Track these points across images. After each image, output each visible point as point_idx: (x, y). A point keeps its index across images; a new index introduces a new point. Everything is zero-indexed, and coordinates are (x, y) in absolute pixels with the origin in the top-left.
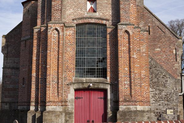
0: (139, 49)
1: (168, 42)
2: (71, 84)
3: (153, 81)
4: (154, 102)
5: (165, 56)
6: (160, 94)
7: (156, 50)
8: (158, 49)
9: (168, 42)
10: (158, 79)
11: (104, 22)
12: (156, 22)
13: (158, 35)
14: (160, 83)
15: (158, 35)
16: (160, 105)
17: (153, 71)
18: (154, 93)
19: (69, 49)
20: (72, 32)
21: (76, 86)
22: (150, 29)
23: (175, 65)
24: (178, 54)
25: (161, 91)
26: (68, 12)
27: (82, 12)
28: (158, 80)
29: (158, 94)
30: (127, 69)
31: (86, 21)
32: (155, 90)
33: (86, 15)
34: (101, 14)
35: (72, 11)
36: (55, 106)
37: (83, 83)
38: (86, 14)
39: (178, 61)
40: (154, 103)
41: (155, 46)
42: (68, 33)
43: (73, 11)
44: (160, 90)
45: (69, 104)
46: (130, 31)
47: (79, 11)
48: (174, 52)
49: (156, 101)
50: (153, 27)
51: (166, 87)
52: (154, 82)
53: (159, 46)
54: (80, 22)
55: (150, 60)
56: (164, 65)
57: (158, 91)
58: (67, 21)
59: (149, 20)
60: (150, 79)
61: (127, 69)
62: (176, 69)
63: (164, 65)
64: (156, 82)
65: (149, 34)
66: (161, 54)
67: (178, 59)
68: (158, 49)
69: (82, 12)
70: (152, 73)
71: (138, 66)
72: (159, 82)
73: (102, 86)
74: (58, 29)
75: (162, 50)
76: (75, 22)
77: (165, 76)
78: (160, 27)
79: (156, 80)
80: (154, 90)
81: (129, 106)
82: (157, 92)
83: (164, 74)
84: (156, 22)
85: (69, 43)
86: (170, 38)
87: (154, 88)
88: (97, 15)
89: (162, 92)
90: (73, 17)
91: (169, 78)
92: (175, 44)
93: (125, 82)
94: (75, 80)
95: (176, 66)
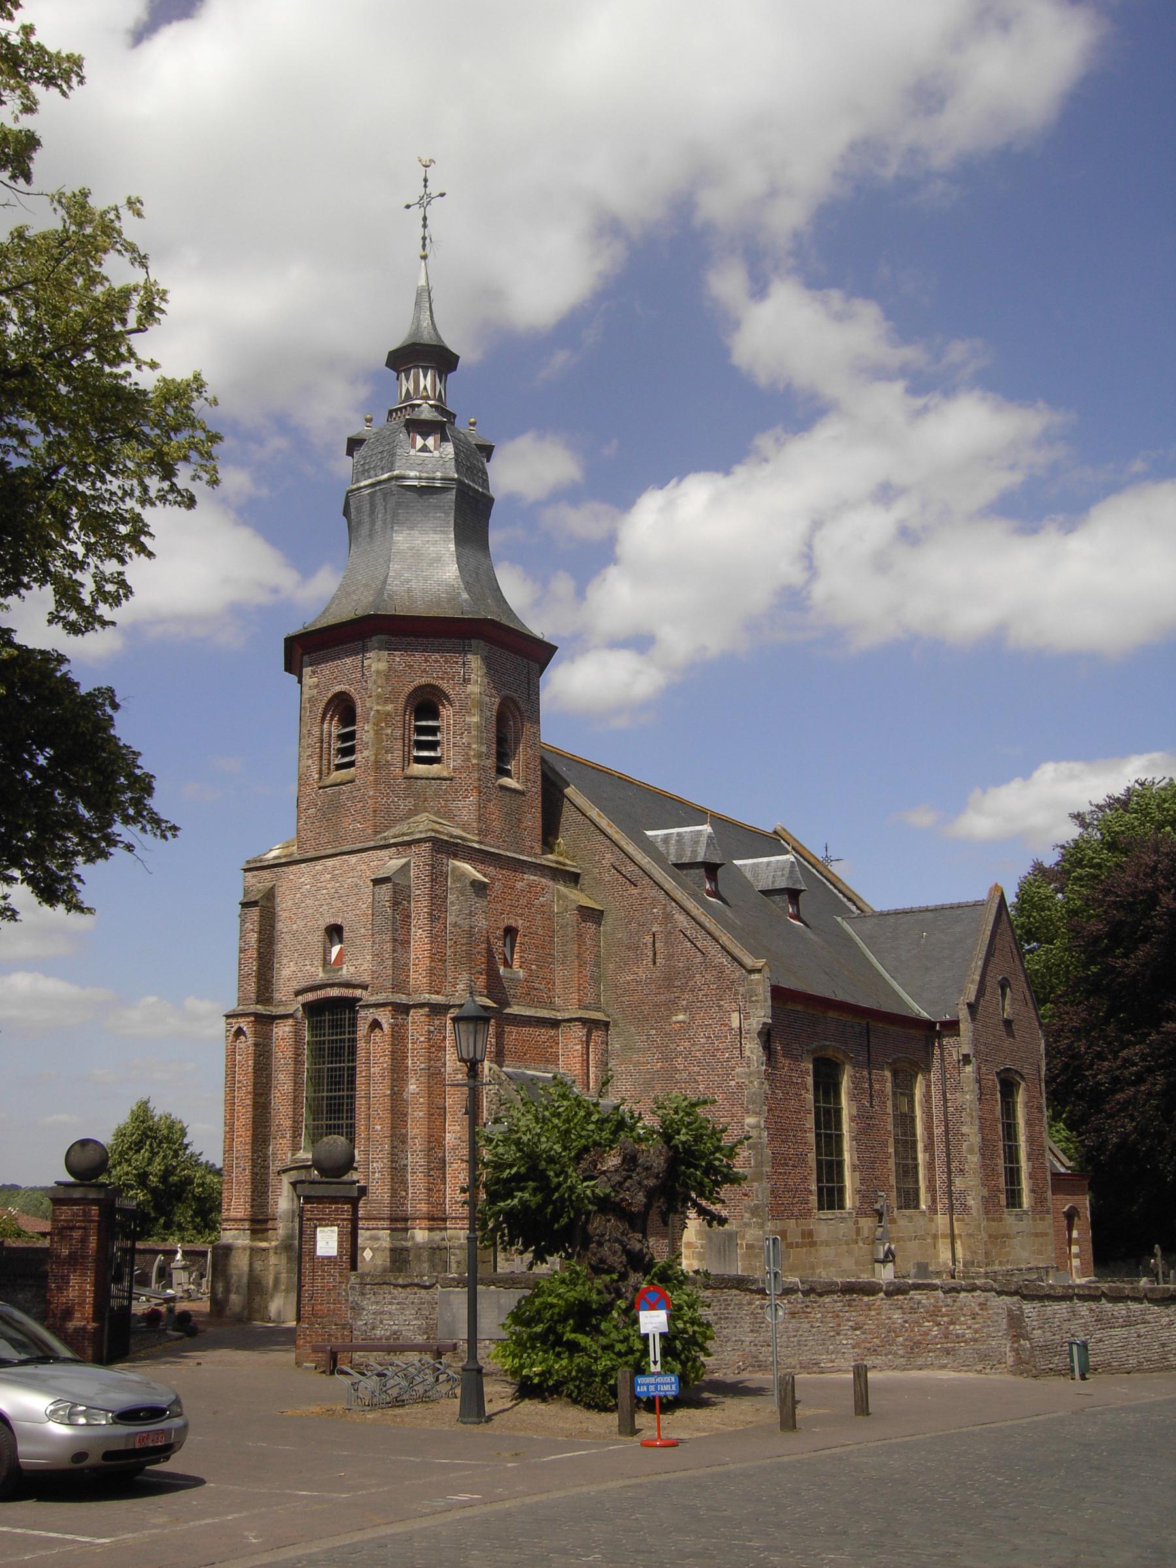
2: (285, 1171)
8: (681, 1017)
11: (358, 993)
12: (676, 916)
19: (281, 1077)
20: (287, 1029)
21: (294, 1175)
23: (738, 1070)
24: (747, 1027)
26: (286, 973)
31: (321, 994)
33: (321, 975)
34: (352, 969)
38: (321, 975)
39: (747, 1053)
41: (671, 1006)
42: (280, 1033)
48: (735, 1024)
53: (684, 1003)
54: (310, 997)
56: (699, 1074)
58: (284, 999)
63: (699, 1074)
65: (654, 963)
71: (421, 1114)
75: (693, 1019)
76: (300, 998)
78: (688, 933)
84: (676, 916)
86: (720, 969)
90: (296, 985)
92: (736, 994)
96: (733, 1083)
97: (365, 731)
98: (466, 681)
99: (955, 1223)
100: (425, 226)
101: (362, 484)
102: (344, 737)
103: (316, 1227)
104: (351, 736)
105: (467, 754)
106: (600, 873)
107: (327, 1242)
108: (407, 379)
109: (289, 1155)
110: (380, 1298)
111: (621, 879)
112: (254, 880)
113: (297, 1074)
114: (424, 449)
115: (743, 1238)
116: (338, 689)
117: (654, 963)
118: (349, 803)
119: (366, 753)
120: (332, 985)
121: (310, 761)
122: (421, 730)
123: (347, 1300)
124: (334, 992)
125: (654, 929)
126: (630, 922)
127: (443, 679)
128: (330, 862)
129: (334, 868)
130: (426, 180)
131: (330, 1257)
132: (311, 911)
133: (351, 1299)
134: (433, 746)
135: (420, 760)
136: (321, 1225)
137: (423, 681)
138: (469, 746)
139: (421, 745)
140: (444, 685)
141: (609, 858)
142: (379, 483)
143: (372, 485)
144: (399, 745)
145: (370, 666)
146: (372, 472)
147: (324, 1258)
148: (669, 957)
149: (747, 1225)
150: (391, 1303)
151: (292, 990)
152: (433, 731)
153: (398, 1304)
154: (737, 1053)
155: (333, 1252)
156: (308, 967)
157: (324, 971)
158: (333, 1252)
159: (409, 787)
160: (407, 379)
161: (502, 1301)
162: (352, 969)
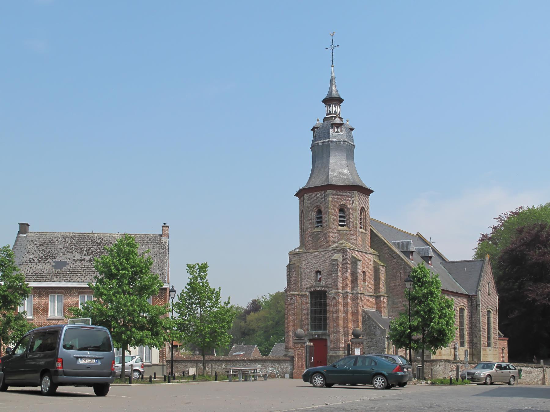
11: (326, 289)
25: (373, 339)
31: (315, 289)
37: (312, 335)
49: (369, 347)
54: (311, 290)
73: (324, 337)
76: (308, 290)
79: (368, 330)
82: (370, 340)
88: (322, 283)
97: (325, 217)
98: (353, 203)
102: (318, 218)
104: (321, 218)
113: (308, 311)
114: (337, 132)
119: (326, 224)
122: (340, 217)
124: (318, 289)
128: (316, 254)
135: (341, 225)
137: (341, 203)
139: (341, 221)
142: (325, 142)
143: (323, 142)
144: (335, 221)
155: (359, 354)
158: (359, 354)
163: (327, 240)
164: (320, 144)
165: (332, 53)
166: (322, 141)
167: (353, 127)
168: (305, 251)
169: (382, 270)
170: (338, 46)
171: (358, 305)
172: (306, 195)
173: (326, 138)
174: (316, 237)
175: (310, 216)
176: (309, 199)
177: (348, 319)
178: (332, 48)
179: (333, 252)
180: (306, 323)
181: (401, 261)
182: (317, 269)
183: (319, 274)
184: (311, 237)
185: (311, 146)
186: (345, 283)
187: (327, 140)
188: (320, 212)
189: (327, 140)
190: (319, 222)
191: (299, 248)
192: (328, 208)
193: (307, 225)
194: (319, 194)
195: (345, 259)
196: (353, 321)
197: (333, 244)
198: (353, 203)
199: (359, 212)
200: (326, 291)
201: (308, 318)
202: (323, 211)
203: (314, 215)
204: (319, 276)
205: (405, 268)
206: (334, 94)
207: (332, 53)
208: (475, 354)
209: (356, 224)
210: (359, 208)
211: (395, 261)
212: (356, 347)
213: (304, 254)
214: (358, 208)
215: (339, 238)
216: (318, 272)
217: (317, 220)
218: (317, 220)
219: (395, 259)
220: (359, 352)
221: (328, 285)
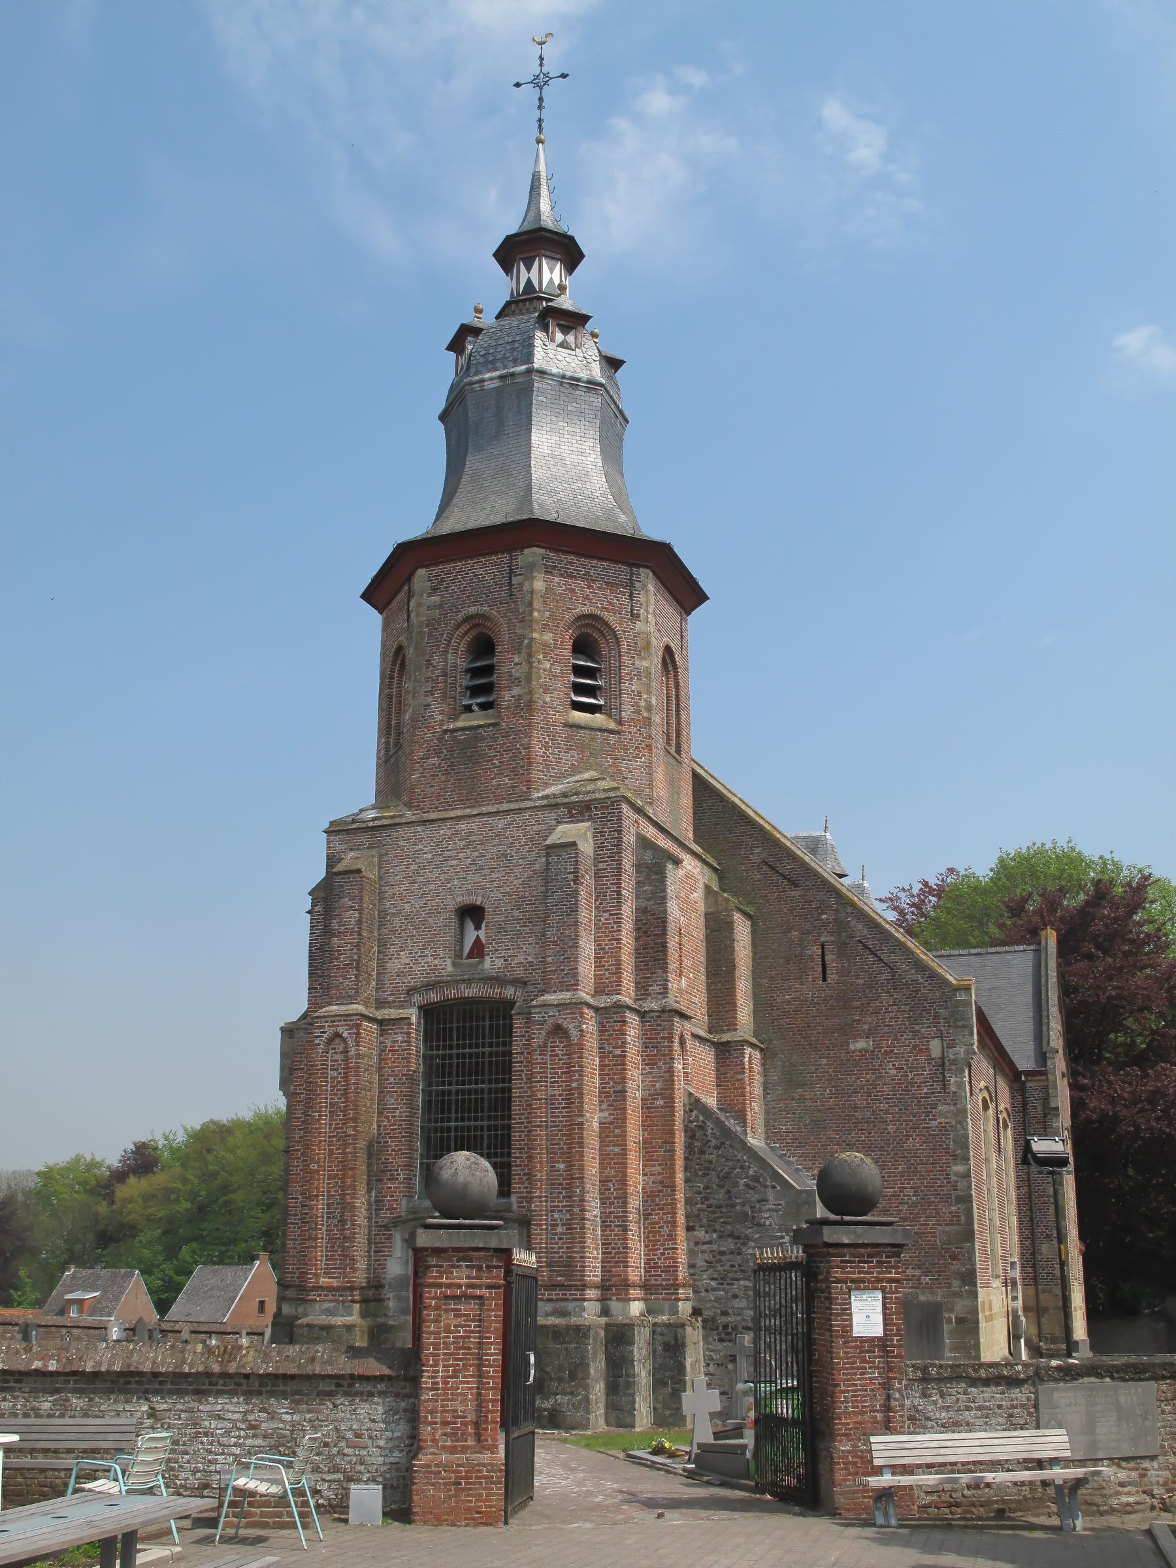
0: (619, 1087)
1: (907, 1008)
3: (711, 1201)
4: (713, 1283)
5: (894, 1072)
6: (739, 1254)
7: (852, 1047)
8: (861, 1044)
9: (907, 1008)
10: (728, 1192)
11: (509, 992)
13: (860, 982)
14: (738, 1208)
15: (860, 982)
16: (735, 1296)
17: (711, 1162)
18: (714, 1247)
22: (827, 958)
24: (952, 1057)
27: (436, 962)
28: (730, 1198)
29: (732, 1253)
30: (562, 1166)
31: (450, 993)
32: (720, 1237)
34: (500, 963)
35: (404, 957)
36: (331, 1301)
38: (450, 969)
39: (953, 1089)
40: (714, 1289)
41: (849, 1031)
43: (408, 961)
44: (738, 1238)
45: (391, 1295)
46: (571, 1026)
47: (429, 959)
49: (722, 1279)
50: (842, 947)
51: (759, 1225)
52: (717, 1207)
53: (866, 1027)
54: (433, 997)
55: (701, 1118)
56: (887, 1112)
57: (730, 1240)
58: (390, 999)
59: (824, 916)
60: (699, 1193)
61: (562, 1166)
62: (942, 1127)
63: (887, 1112)
64: (721, 1207)
65: (824, 979)
66: (877, 1062)
67: (952, 1080)
68: (861, 1044)
69: (436, 962)
70: (708, 1169)
72: (733, 1206)
74: (345, 1035)
75: (877, 1046)
76: (416, 999)
77: (756, 1179)
80: (715, 1235)
81: (563, 1304)
82: (731, 1244)
83: (751, 1172)
85: (391, 1079)
87: (715, 1231)
88: (489, 964)
89: (744, 1244)
91: (774, 1187)
92: (936, 1017)
93: (556, 1216)
94: (409, 1212)
95: (941, 1114)
96: (934, 1123)
98: (635, 617)
99: (1042, 1296)
100: (540, 107)
101: (487, 376)
103: (850, 1290)
104: (489, 670)
105: (637, 704)
106: (747, 871)
107: (867, 1315)
108: (529, 269)
109: (404, 1202)
110: (949, 1400)
111: (777, 879)
112: (343, 847)
113: (411, 1097)
115: (951, 1310)
116: (472, 610)
117: (824, 979)
118: (492, 753)
119: (516, 691)
120: (468, 982)
121: (430, 699)
122: (578, 671)
123: (902, 1406)
124: (472, 992)
125: (823, 939)
126: (789, 930)
127: (608, 610)
128: (463, 826)
129: (470, 832)
130: (541, 58)
131: (871, 1340)
132: (433, 887)
133: (908, 1403)
134: (590, 691)
135: (578, 706)
136: (858, 1289)
137: (586, 610)
138: (639, 695)
139: (579, 689)
140: (607, 616)
141: (758, 854)
142: (513, 375)
143: (501, 377)
145: (521, 585)
146: (498, 365)
147: (863, 1340)
148: (843, 973)
149: (955, 1294)
150: (968, 1409)
151: (403, 987)
152: (590, 673)
153: (979, 1408)
154: (938, 1087)
155: (878, 1331)
156: (429, 959)
157: (454, 964)
158: (878, 1331)
159: (570, 738)
160: (529, 269)
161: (1122, 1399)
162: (500, 963)
163: (520, 767)
164: (489, 385)
165: (541, 99)
166: (494, 374)
167: (618, 356)
168: (409, 815)
169: (742, 930)
170: (564, 76)
171: (671, 1071)
172: (421, 572)
173: (515, 362)
174: (465, 752)
175: (437, 660)
176: (434, 590)
177: (623, 1136)
178: (540, 82)
179: (551, 816)
180: (402, 1160)
181: (821, 895)
182: (467, 900)
183: (470, 926)
184: (438, 752)
185: (442, 406)
186: (606, 958)
187: (523, 368)
188: (484, 646)
189: (523, 368)
190: (475, 691)
191: (374, 807)
192: (526, 620)
193: (422, 700)
194: (484, 570)
195: (610, 846)
196: (648, 1148)
197: (547, 785)
198: (635, 617)
199: (658, 660)
200: (511, 1004)
201: (410, 1134)
202: (503, 640)
203: (458, 658)
204: (471, 935)
205: (840, 926)
206: (547, 219)
207: (541, 99)
208: (1046, 1310)
209: (649, 708)
210: (657, 644)
211: (796, 893)
212: (859, 1284)
213: (403, 832)
214: (654, 641)
215: (572, 758)
216: (472, 913)
217: (466, 681)
218: (466, 681)
219: (794, 884)
220: (857, 1319)
221: (520, 973)
